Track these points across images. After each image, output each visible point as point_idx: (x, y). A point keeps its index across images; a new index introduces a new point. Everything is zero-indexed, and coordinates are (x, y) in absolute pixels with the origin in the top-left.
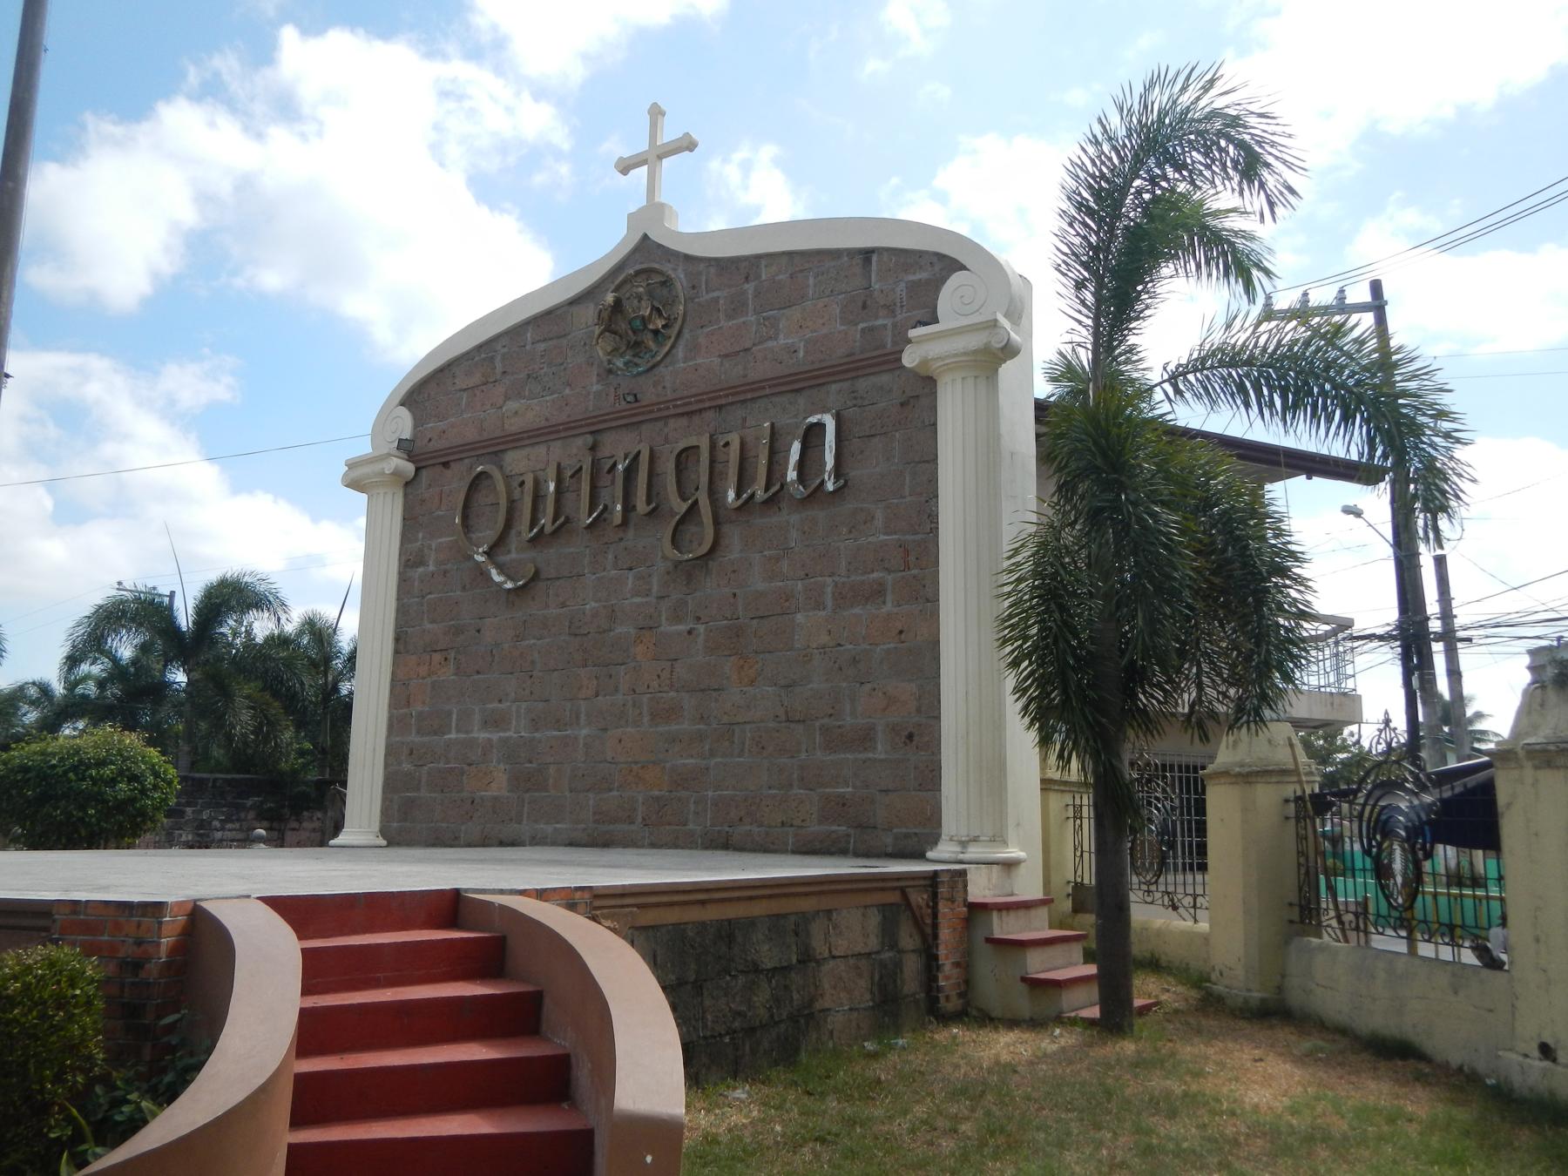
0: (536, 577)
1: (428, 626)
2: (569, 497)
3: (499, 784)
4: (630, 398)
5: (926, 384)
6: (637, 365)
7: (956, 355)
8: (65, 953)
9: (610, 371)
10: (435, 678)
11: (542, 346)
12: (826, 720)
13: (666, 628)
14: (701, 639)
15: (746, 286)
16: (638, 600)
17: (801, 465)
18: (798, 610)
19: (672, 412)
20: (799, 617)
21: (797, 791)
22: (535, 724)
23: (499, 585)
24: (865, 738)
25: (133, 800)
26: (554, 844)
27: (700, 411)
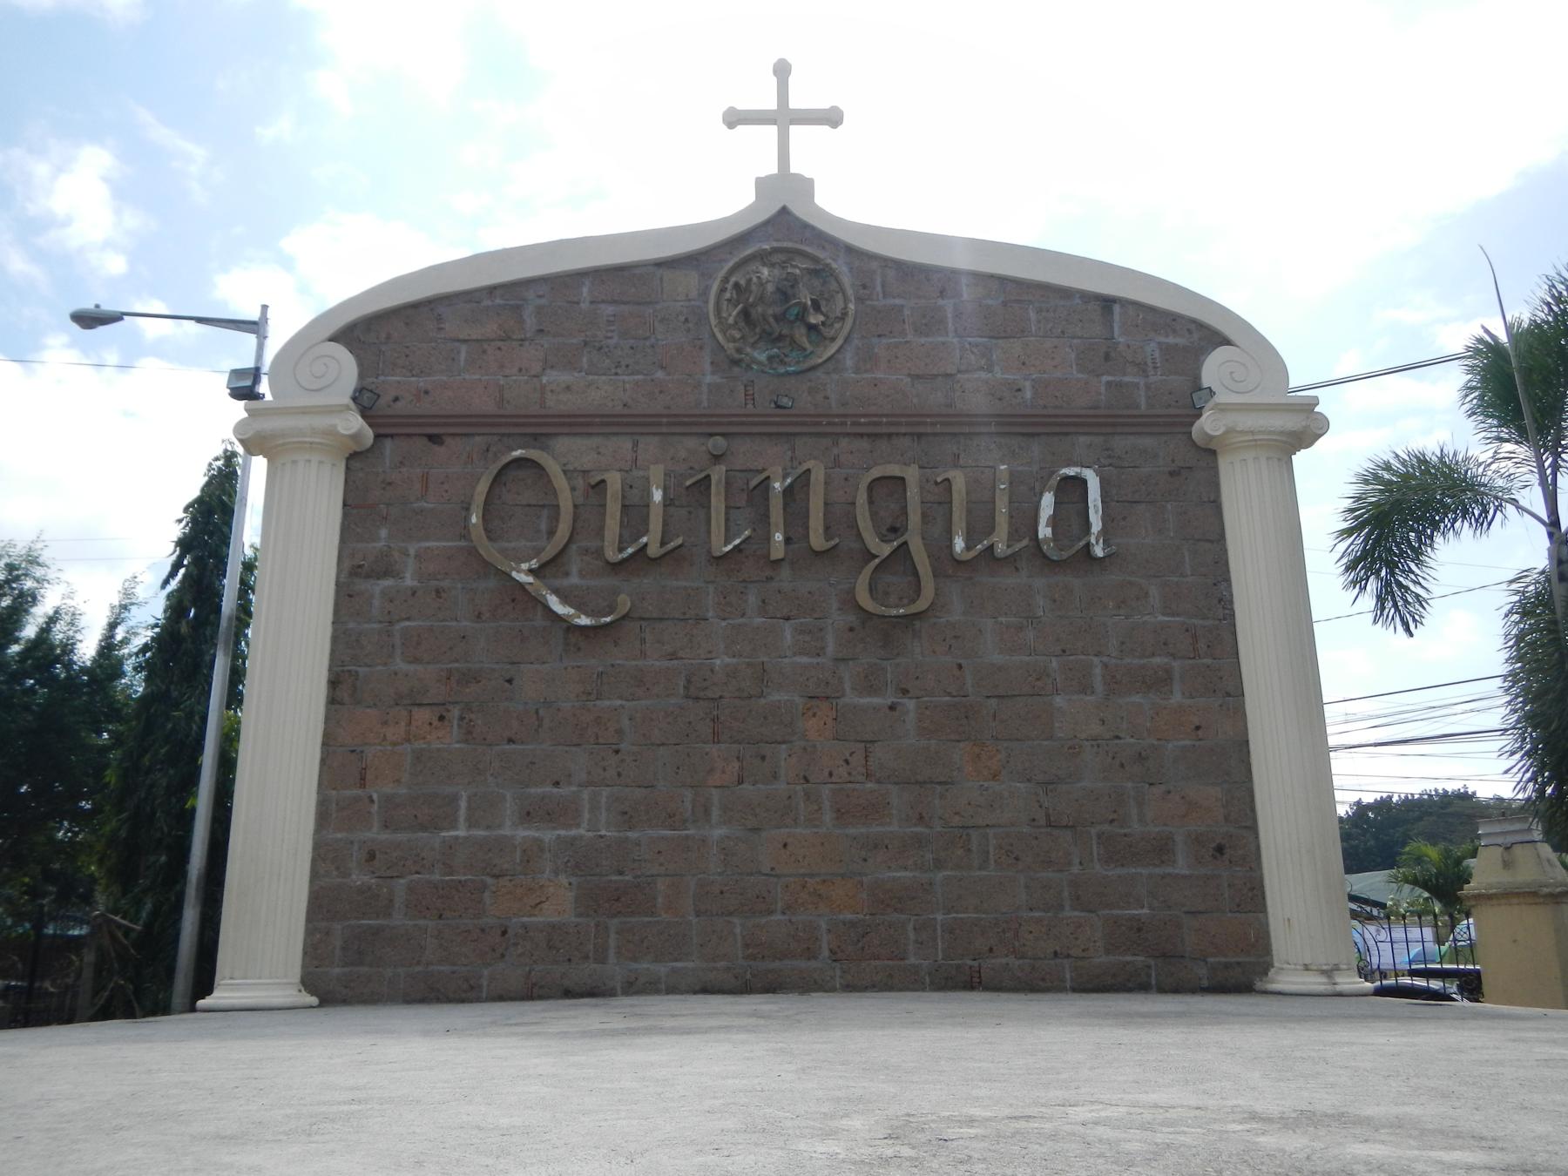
1: (400, 665)
3: (559, 903)
4: (785, 401)
5: (1209, 454)
6: (782, 362)
7: (1270, 433)
9: (736, 362)
12: (1106, 827)
13: (851, 698)
15: (940, 302)
16: (805, 660)
17: (1054, 521)
19: (849, 429)
20: (1059, 701)
22: (627, 818)
24: (1162, 849)
26: (672, 990)
27: (890, 435)
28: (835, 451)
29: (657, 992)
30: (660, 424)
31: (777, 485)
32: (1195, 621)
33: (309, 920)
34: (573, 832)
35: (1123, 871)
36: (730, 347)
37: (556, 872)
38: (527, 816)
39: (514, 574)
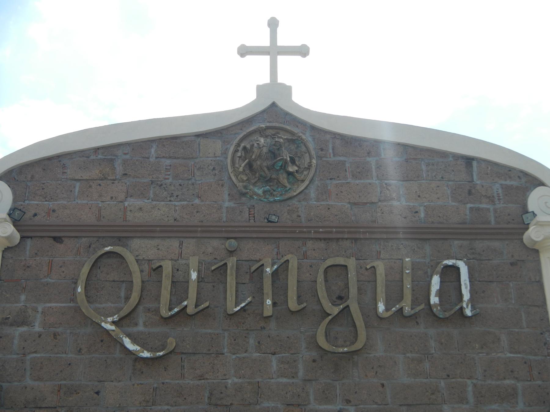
4: (273, 218)
9: (244, 194)
11: (168, 162)
15: (368, 159)
16: (284, 380)
17: (440, 293)
19: (312, 236)
27: (338, 239)
28: (304, 249)
30: (196, 232)
31: (268, 270)
32: (532, 357)
36: (240, 185)
39: (103, 324)
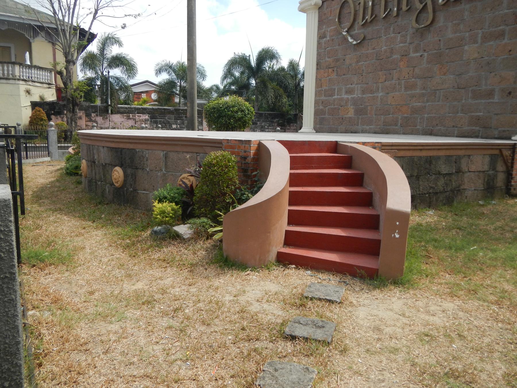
0: (364, 38)
1: (327, 59)
2: (377, 7)
3: (351, 113)
8: (226, 153)
10: (330, 77)
12: (474, 88)
13: (412, 55)
14: (425, 59)
16: (402, 45)
18: (466, 44)
20: (466, 48)
21: (460, 114)
22: (363, 92)
23: (351, 43)
24: (490, 94)
25: (242, 117)
26: (369, 133)
29: (366, 133)
33: (314, 116)
34: (354, 96)
35: (477, 101)
37: (351, 105)
38: (347, 93)
